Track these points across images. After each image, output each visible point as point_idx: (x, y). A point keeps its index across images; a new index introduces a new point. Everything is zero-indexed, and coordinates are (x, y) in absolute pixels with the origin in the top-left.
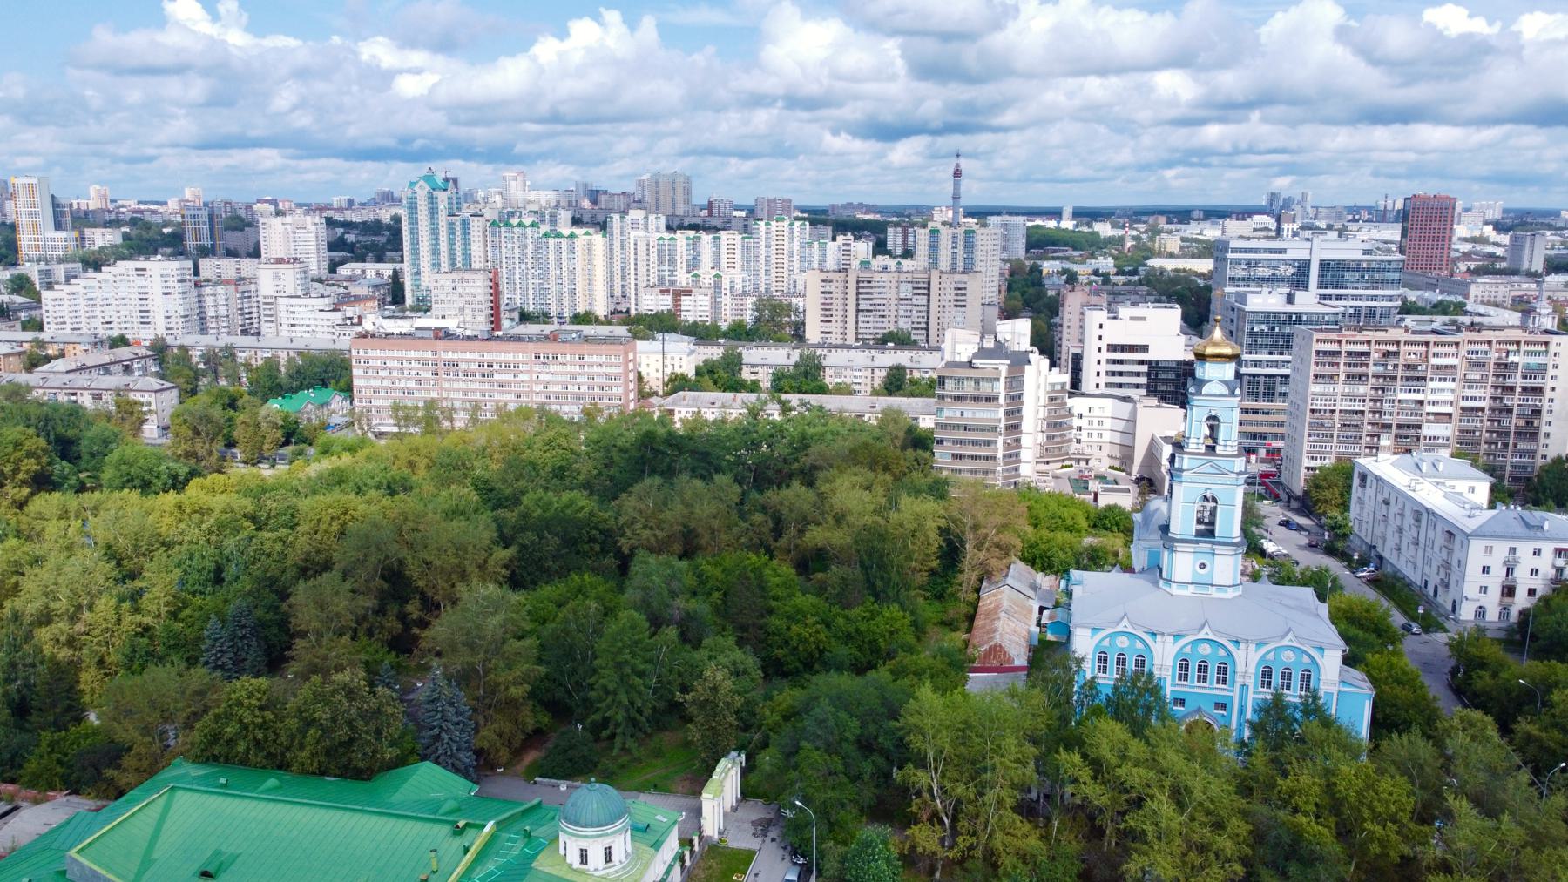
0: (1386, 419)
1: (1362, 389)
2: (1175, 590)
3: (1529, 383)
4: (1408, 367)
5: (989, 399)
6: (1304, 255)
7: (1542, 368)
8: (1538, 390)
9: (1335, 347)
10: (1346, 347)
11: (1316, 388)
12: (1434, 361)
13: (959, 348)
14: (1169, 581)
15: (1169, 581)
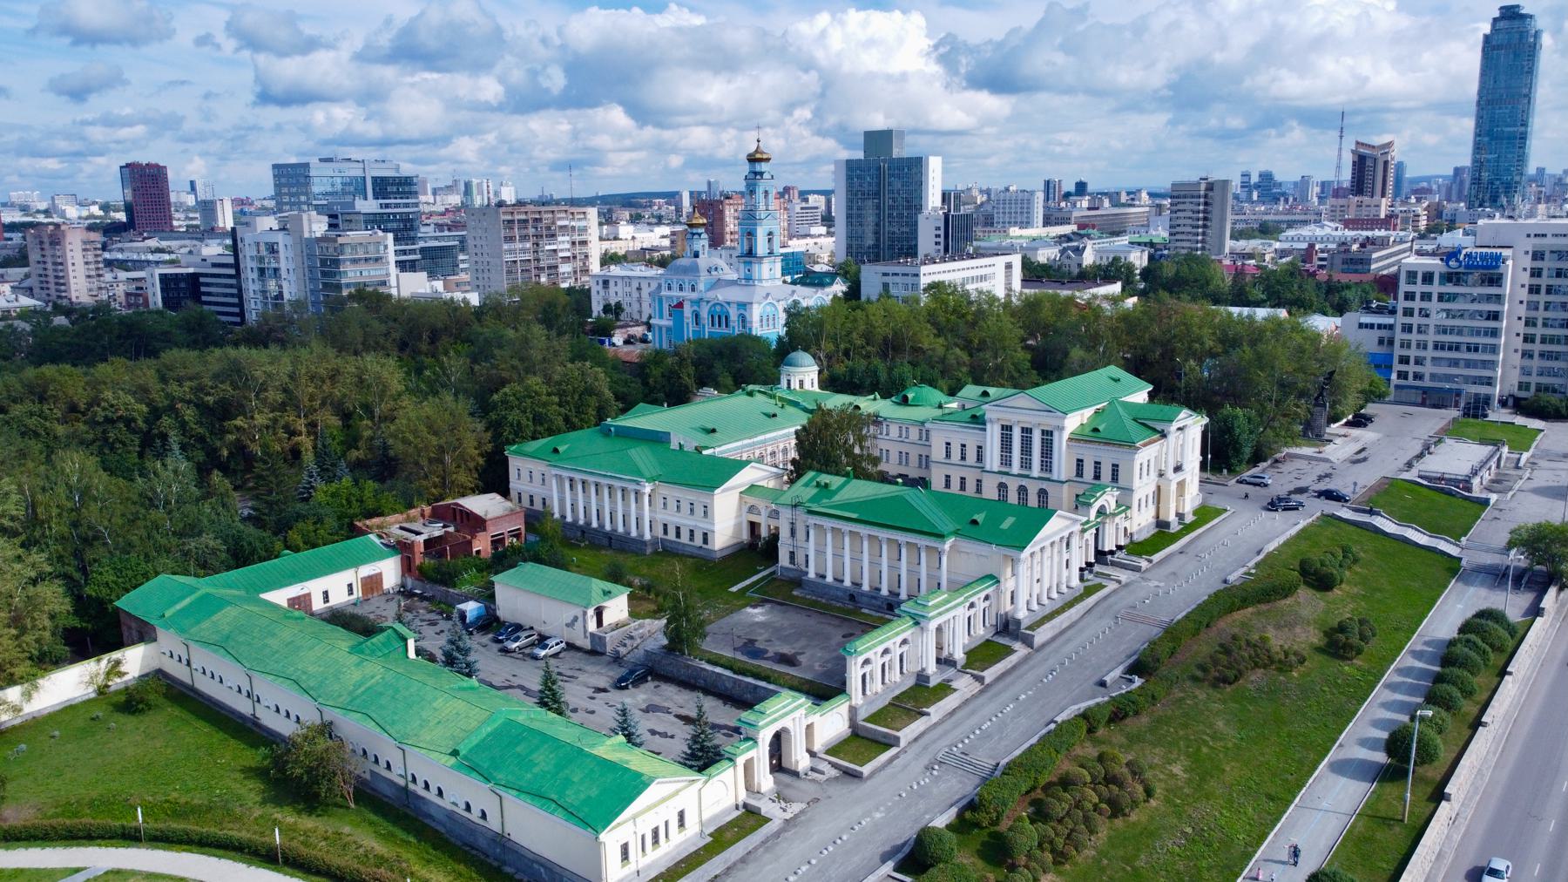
0: (542, 264)
1: (528, 245)
2: (765, 284)
3: (583, 238)
4: (549, 228)
5: (377, 260)
6: (359, 173)
7: (584, 230)
8: (584, 243)
9: (509, 217)
10: (517, 217)
11: (506, 247)
12: (560, 223)
13: (315, 227)
14: (760, 280)
15: (760, 280)
